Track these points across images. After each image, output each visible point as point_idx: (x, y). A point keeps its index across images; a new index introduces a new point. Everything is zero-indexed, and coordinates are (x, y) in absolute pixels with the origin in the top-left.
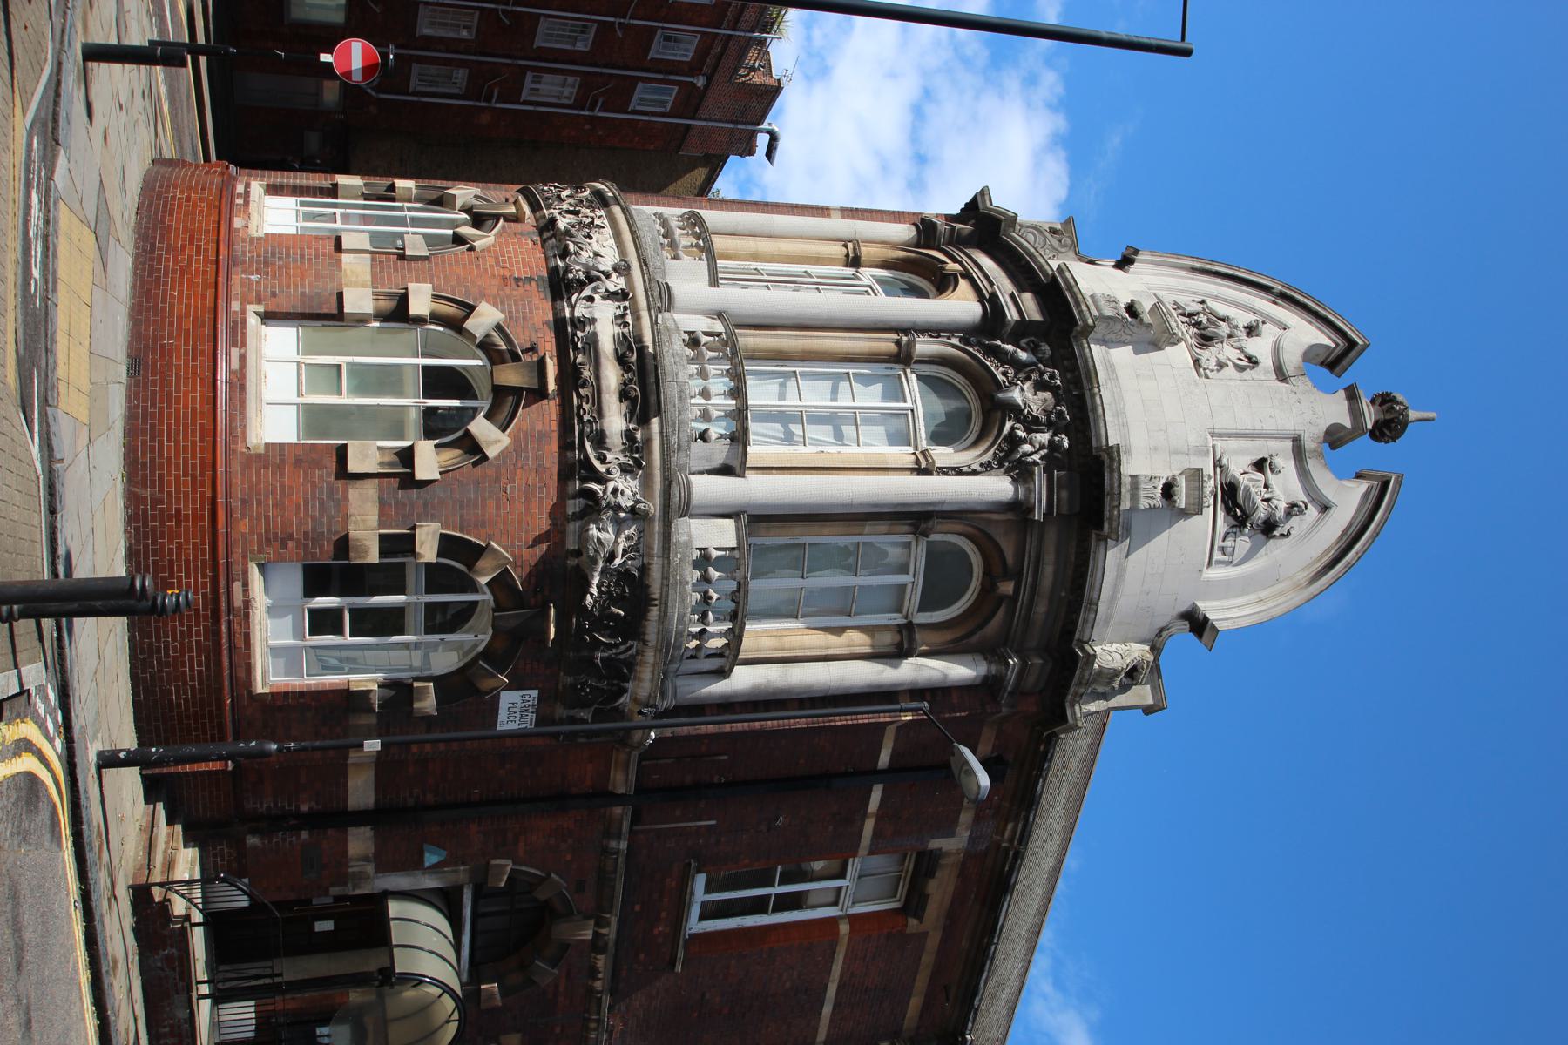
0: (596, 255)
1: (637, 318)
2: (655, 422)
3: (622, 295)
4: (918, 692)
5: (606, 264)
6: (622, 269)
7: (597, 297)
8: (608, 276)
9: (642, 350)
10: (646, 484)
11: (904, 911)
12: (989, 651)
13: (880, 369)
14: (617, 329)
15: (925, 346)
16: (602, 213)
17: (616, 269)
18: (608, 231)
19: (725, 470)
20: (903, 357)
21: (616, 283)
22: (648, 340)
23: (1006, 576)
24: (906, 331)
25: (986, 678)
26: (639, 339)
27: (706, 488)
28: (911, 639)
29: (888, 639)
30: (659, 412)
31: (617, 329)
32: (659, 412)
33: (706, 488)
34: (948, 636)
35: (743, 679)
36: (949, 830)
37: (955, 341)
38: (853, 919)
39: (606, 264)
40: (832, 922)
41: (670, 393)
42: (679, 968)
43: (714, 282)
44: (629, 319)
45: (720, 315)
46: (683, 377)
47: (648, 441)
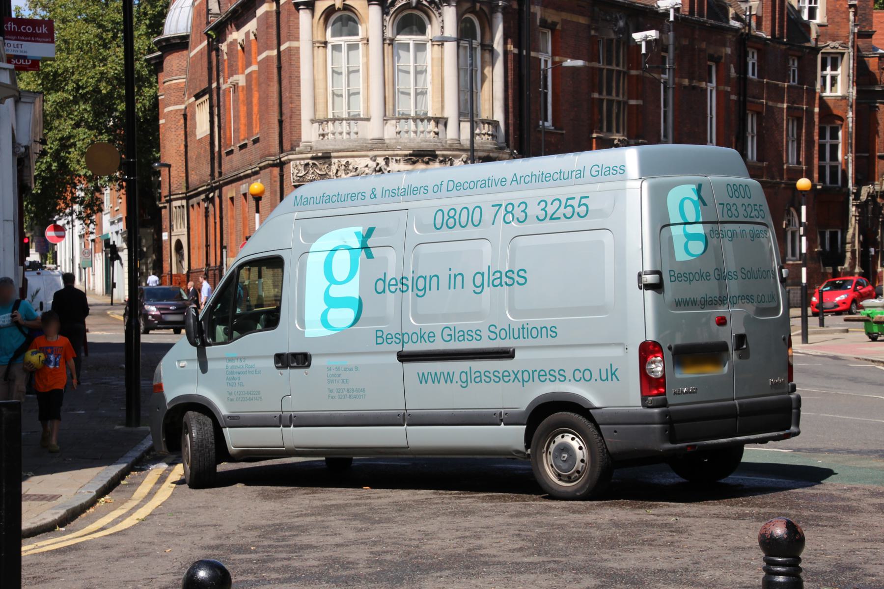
0: (367, 166)
1: (397, 155)
2: (437, 153)
3: (387, 160)
4: (505, 43)
5: (372, 164)
6: (374, 159)
7: (388, 169)
8: (378, 164)
9: (410, 155)
10: (457, 157)
11: (553, 31)
12: (494, 9)
13: (395, 51)
14: (402, 162)
15: (389, 34)
16: (333, 160)
17: (375, 161)
18: (348, 159)
19: (446, 125)
20: (392, 41)
21: (381, 161)
22: (407, 152)
23: (474, 6)
24: (384, 40)
25: (503, 14)
26: (406, 156)
27: (451, 133)
28: (489, 46)
29: (487, 56)
30: (434, 151)
31: (402, 162)
32: (434, 151)
33: (451, 133)
34: (487, 29)
35: (499, 116)
36: (535, 15)
37: (388, 18)
38: (554, 54)
39: (372, 164)
40: (553, 63)
41: (425, 146)
42: (564, 132)
43: (368, 119)
44: (398, 158)
45: (386, 120)
46: (419, 140)
47: (443, 156)
